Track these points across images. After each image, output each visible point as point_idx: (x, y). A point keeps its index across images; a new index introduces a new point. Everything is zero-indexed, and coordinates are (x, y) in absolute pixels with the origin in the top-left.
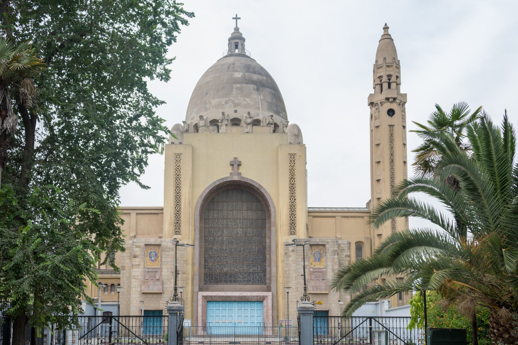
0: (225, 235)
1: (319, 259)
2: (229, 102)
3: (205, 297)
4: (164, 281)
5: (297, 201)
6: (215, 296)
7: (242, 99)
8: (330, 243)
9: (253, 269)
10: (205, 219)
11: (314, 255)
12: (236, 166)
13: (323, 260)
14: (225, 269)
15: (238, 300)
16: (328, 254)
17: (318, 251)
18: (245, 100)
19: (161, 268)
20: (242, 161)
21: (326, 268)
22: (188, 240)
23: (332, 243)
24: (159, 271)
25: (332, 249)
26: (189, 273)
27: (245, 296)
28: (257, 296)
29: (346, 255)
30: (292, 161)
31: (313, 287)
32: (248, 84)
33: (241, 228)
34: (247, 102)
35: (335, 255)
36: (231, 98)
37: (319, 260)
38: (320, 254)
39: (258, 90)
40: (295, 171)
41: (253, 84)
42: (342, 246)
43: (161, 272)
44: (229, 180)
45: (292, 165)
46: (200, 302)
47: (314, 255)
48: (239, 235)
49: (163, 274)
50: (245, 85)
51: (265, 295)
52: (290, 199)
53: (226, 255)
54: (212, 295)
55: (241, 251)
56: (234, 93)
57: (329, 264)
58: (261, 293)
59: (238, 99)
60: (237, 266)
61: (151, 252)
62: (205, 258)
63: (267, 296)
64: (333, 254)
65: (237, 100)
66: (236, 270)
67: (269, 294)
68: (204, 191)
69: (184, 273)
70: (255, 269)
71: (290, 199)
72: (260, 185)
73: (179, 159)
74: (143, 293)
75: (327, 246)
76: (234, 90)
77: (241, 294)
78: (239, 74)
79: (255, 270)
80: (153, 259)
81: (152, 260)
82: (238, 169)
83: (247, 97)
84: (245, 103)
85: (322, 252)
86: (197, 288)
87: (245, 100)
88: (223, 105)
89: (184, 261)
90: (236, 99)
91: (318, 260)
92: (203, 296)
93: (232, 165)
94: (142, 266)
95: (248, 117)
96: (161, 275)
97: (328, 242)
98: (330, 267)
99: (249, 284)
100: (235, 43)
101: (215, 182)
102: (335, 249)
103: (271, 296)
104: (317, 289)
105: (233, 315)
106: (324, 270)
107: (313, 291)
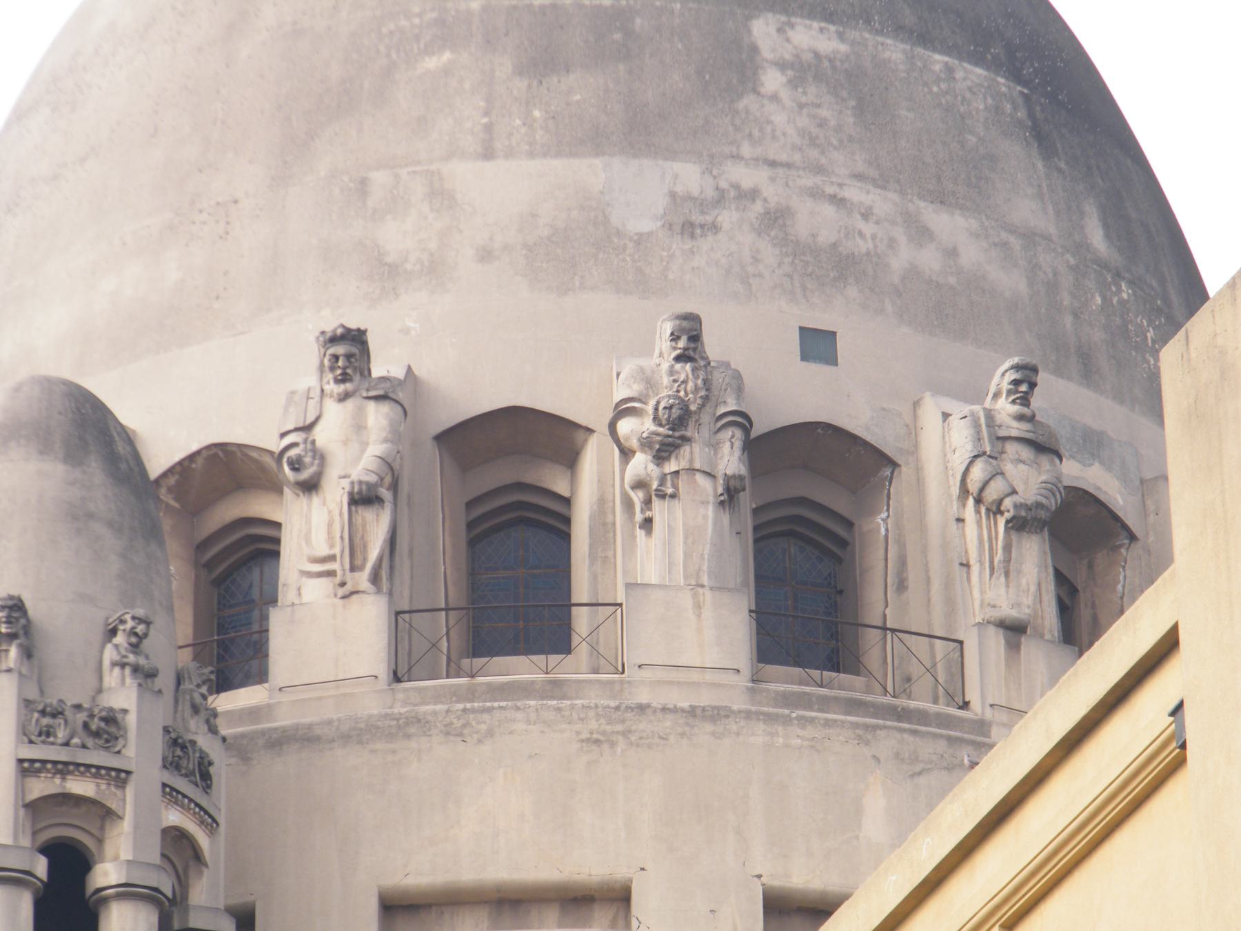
2: (727, 217)
7: (882, 202)
18: (921, 234)
32: (924, 39)
34: (952, 253)
36: (747, 176)
41: (978, 60)
50: (894, 51)
56: (779, 119)
59: (838, 201)
65: (829, 210)
76: (772, 80)
83: (941, 199)
84: (930, 260)
87: (921, 234)
88: (641, 240)
90: (815, 194)
95: (1017, 429)
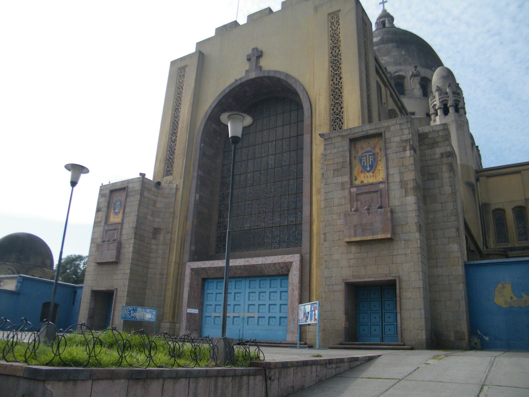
0: (249, 171)
1: (371, 167)
3: (195, 271)
4: (123, 242)
5: (344, 80)
6: (210, 268)
8: (392, 128)
9: (290, 219)
10: (224, 152)
11: (361, 161)
12: (254, 59)
13: (381, 166)
14: (247, 226)
15: (245, 274)
16: (389, 151)
17: (369, 149)
19: (122, 223)
20: (264, 49)
21: (387, 180)
22: (180, 181)
23: (398, 127)
24: (120, 227)
25: (397, 139)
26: (175, 231)
27: (253, 265)
28: (275, 264)
29: (442, 154)
30: (335, 23)
31: (355, 226)
32: (386, 44)
33: (272, 155)
35: (405, 150)
37: (373, 168)
38: (374, 154)
39: (398, 47)
40: (340, 35)
42: (430, 136)
43: (122, 229)
44: (243, 80)
45: (334, 28)
46: (187, 281)
47: (361, 161)
48: (270, 166)
49: (124, 231)
50: (382, 46)
51: (287, 261)
52: (332, 80)
53: (249, 202)
54: (205, 266)
55: (271, 192)
57: (391, 171)
58: (280, 256)
60: (264, 218)
61: (117, 202)
62: (220, 211)
63: (291, 263)
64: (401, 149)
66: (263, 225)
67: (295, 259)
68: (211, 106)
69: (168, 233)
70: (293, 219)
71: (332, 80)
72: (287, 75)
73: (183, 74)
74: (99, 264)
75: (388, 135)
77: (248, 262)
78: (377, 39)
79: (292, 221)
80: (117, 211)
81: (115, 213)
82: (257, 62)
83: (385, 56)
85: (377, 150)
86: (187, 256)
89: (171, 213)
91: (368, 169)
92: (192, 270)
93: (249, 60)
94: (103, 222)
96: (121, 234)
97: (388, 127)
98: (396, 178)
99: (282, 248)
100: (382, 22)
101: (224, 91)
102: (405, 137)
103: (298, 263)
104: (363, 230)
105: (242, 303)
106: (382, 186)
107: (355, 236)
